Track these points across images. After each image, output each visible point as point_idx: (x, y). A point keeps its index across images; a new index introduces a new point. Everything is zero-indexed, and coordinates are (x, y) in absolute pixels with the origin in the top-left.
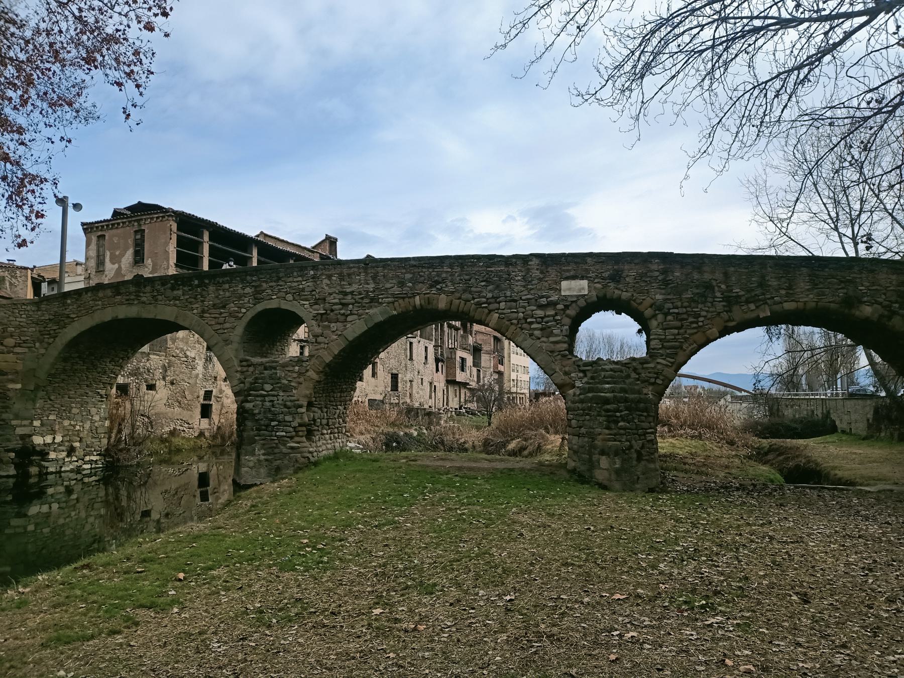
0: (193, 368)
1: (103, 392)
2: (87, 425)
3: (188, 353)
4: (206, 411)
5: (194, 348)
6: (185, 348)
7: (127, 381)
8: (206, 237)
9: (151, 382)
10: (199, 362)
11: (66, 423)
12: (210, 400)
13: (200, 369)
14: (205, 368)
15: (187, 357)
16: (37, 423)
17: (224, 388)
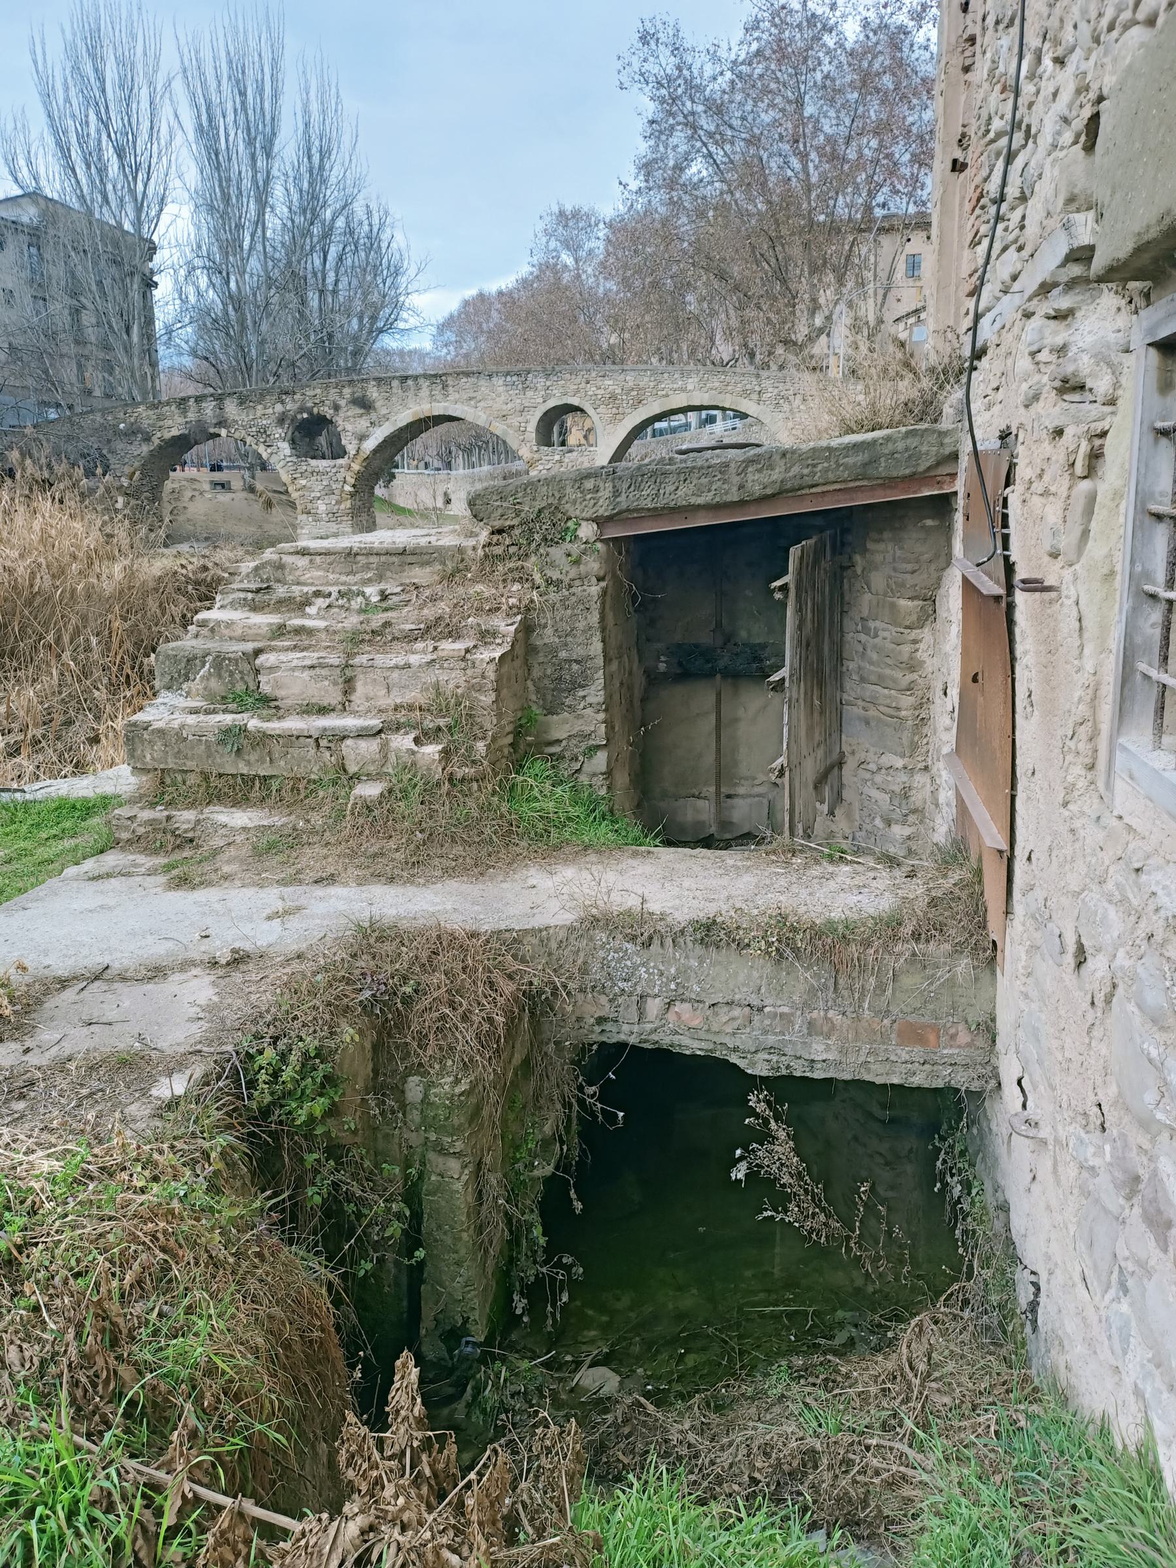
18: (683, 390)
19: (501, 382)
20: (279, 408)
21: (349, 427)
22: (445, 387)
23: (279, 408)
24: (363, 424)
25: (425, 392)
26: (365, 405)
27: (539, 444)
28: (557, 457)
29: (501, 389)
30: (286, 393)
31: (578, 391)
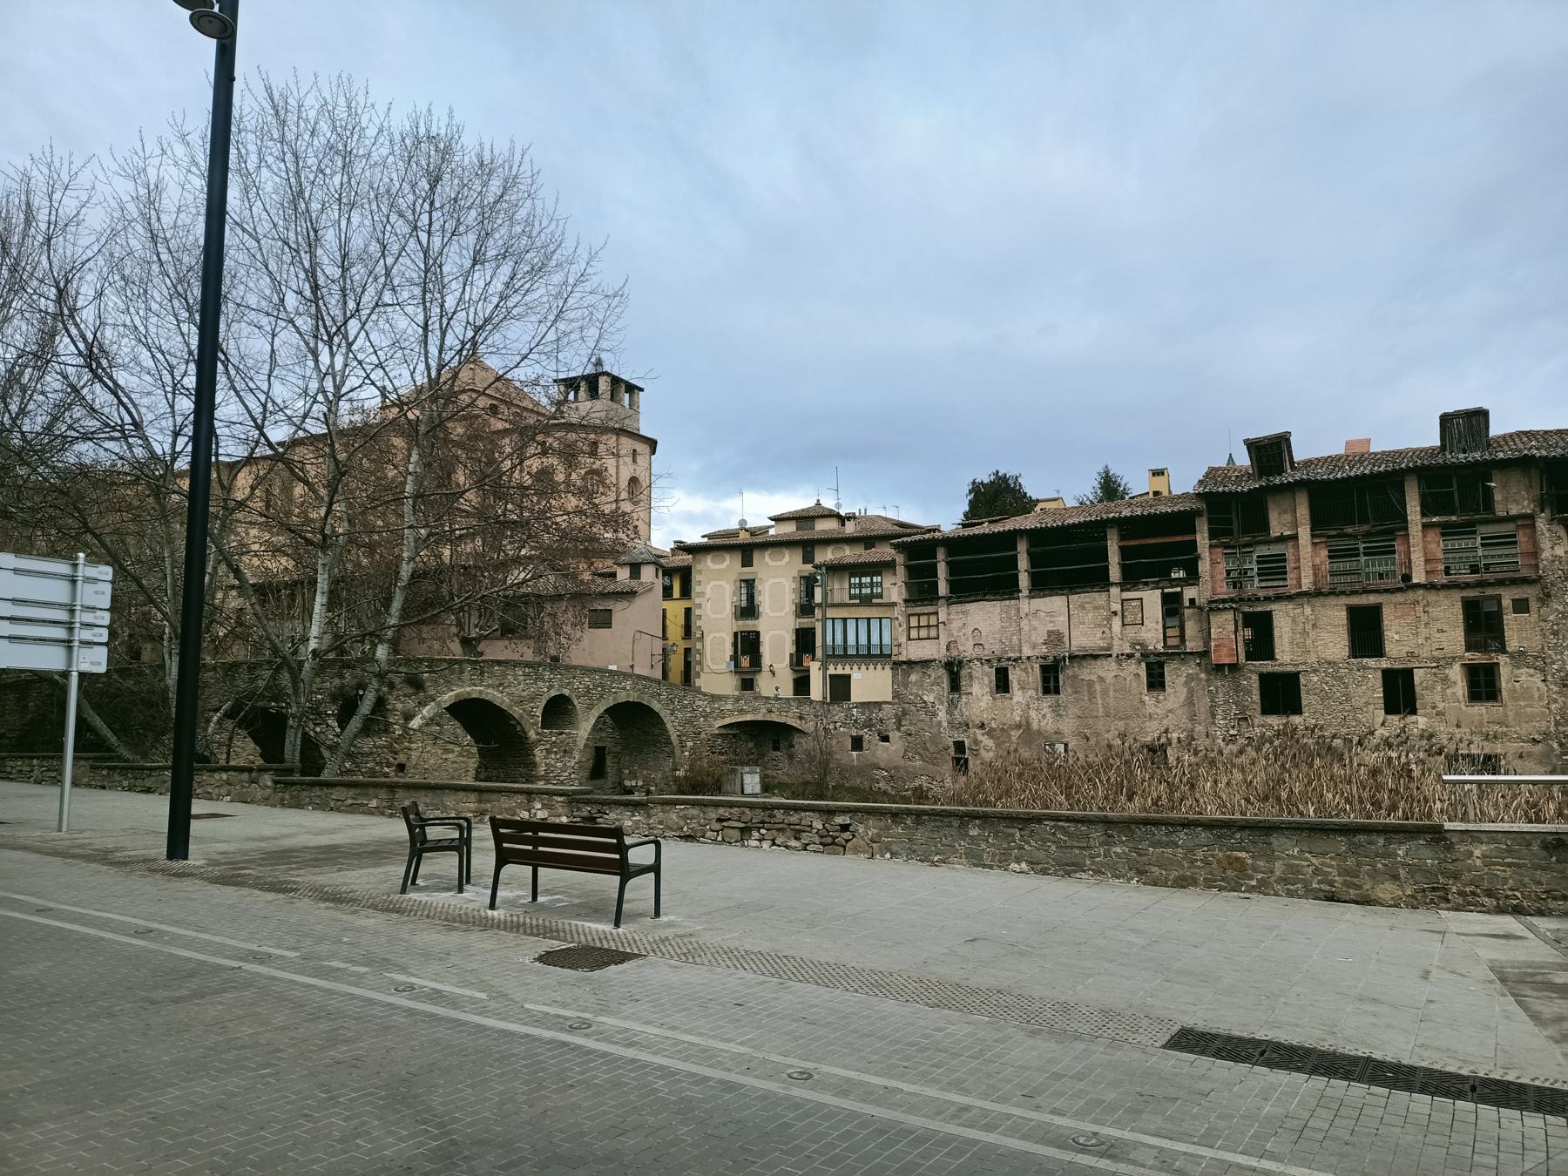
0: (935, 714)
1: (667, 749)
2: (659, 775)
3: (925, 698)
4: (961, 764)
5: (932, 691)
6: (920, 692)
7: (861, 733)
8: (941, 554)
9: (885, 733)
10: (940, 707)
11: (645, 772)
12: (964, 753)
13: (942, 715)
14: (950, 713)
15: (925, 702)
16: (627, 772)
17: (980, 738)
18: (624, 689)
19: (521, 673)
20: (337, 681)
21: (399, 706)
22: (482, 674)
23: (337, 681)
24: (411, 704)
25: (466, 676)
26: (417, 684)
27: (543, 728)
28: (554, 738)
29: (522, 678)
30: (349, 667)
31: (568, 684)
